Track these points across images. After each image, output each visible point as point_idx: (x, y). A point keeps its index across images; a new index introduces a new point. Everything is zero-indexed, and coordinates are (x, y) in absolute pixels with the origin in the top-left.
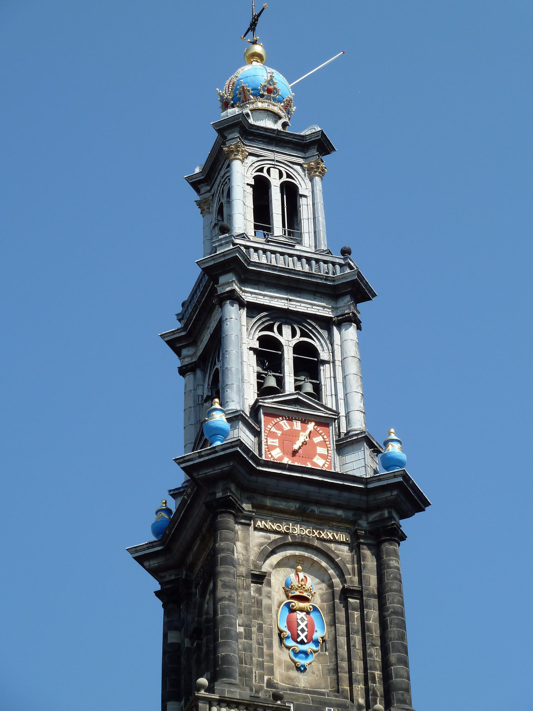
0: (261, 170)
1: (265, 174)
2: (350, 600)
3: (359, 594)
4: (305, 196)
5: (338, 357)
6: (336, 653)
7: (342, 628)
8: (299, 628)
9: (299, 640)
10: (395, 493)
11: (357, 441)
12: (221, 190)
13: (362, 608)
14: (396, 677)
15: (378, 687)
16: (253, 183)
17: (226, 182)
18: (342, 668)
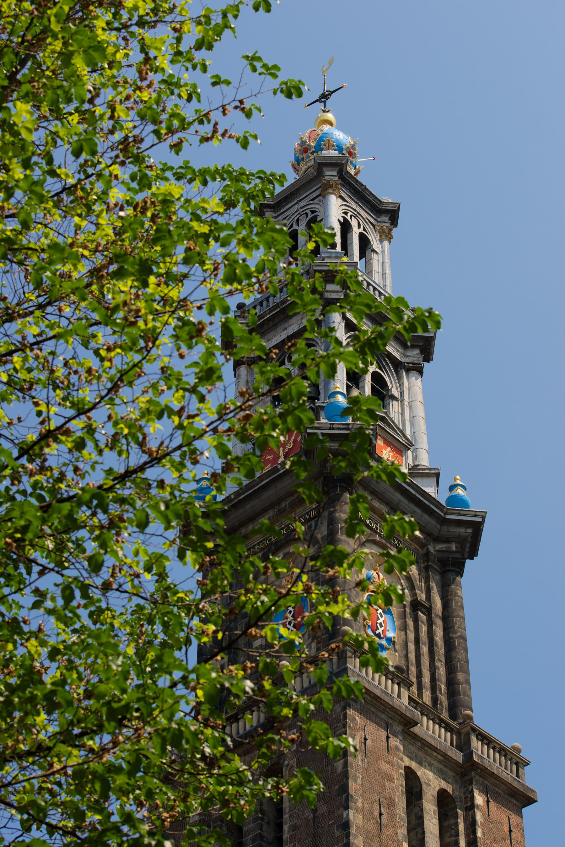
0: (346, 213)
1: (349, 218)
2: (420, 613)
3: (429, 611)
4: (377, 253)
5: (406, 397)
6: (407, 656)
7: (411, 636)
8: (379, 622)
9: (377, 632)
10: (470, 531)
11: (428, 475)
12: (296, 218)
13: (430, 624)
14: (464, 695)
15: (443, 698)
16: (342, 221)
17: (307, 214)
18: (412, 672)
